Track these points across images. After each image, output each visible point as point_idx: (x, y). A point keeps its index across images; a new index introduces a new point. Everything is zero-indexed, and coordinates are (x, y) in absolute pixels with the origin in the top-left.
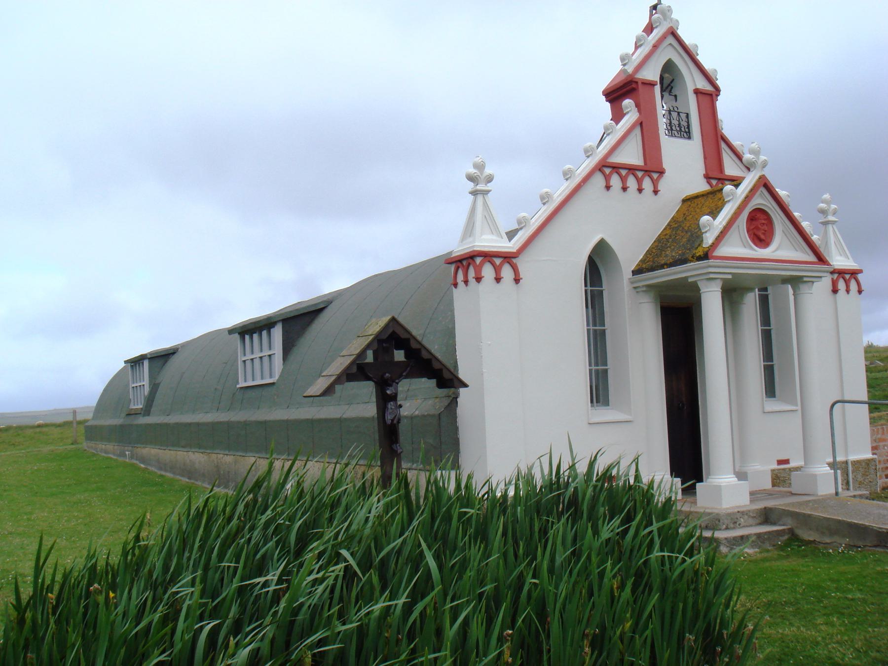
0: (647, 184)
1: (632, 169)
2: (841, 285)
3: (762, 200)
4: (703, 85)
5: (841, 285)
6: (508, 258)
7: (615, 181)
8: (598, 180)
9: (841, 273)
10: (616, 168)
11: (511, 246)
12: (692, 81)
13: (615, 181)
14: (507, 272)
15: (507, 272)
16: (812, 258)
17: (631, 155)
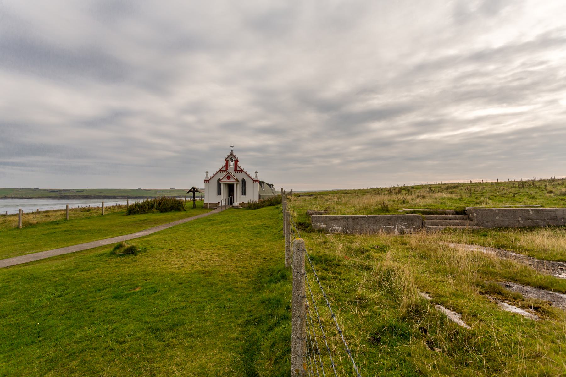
0: (226, 172)
1: (224, 171)
2: (255, 182)
3: (229, 175)
4: (235, 160)
5: (255, 182)
6: (208, 181)
7: (222, 172)
8: (220, 172)
9: (255, 181)
10: (222, 171)
11: (209, 179)
12: (234, 159)
13: (222, 172)
14: (208, 182)
15: (208, 182)
16: (235, 180)
17: (224, 169)
